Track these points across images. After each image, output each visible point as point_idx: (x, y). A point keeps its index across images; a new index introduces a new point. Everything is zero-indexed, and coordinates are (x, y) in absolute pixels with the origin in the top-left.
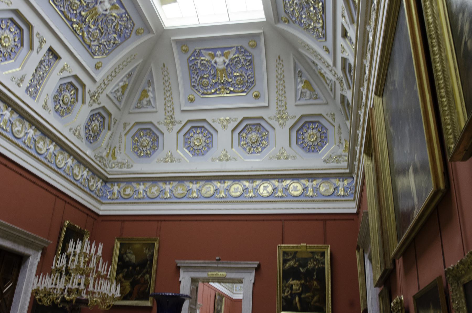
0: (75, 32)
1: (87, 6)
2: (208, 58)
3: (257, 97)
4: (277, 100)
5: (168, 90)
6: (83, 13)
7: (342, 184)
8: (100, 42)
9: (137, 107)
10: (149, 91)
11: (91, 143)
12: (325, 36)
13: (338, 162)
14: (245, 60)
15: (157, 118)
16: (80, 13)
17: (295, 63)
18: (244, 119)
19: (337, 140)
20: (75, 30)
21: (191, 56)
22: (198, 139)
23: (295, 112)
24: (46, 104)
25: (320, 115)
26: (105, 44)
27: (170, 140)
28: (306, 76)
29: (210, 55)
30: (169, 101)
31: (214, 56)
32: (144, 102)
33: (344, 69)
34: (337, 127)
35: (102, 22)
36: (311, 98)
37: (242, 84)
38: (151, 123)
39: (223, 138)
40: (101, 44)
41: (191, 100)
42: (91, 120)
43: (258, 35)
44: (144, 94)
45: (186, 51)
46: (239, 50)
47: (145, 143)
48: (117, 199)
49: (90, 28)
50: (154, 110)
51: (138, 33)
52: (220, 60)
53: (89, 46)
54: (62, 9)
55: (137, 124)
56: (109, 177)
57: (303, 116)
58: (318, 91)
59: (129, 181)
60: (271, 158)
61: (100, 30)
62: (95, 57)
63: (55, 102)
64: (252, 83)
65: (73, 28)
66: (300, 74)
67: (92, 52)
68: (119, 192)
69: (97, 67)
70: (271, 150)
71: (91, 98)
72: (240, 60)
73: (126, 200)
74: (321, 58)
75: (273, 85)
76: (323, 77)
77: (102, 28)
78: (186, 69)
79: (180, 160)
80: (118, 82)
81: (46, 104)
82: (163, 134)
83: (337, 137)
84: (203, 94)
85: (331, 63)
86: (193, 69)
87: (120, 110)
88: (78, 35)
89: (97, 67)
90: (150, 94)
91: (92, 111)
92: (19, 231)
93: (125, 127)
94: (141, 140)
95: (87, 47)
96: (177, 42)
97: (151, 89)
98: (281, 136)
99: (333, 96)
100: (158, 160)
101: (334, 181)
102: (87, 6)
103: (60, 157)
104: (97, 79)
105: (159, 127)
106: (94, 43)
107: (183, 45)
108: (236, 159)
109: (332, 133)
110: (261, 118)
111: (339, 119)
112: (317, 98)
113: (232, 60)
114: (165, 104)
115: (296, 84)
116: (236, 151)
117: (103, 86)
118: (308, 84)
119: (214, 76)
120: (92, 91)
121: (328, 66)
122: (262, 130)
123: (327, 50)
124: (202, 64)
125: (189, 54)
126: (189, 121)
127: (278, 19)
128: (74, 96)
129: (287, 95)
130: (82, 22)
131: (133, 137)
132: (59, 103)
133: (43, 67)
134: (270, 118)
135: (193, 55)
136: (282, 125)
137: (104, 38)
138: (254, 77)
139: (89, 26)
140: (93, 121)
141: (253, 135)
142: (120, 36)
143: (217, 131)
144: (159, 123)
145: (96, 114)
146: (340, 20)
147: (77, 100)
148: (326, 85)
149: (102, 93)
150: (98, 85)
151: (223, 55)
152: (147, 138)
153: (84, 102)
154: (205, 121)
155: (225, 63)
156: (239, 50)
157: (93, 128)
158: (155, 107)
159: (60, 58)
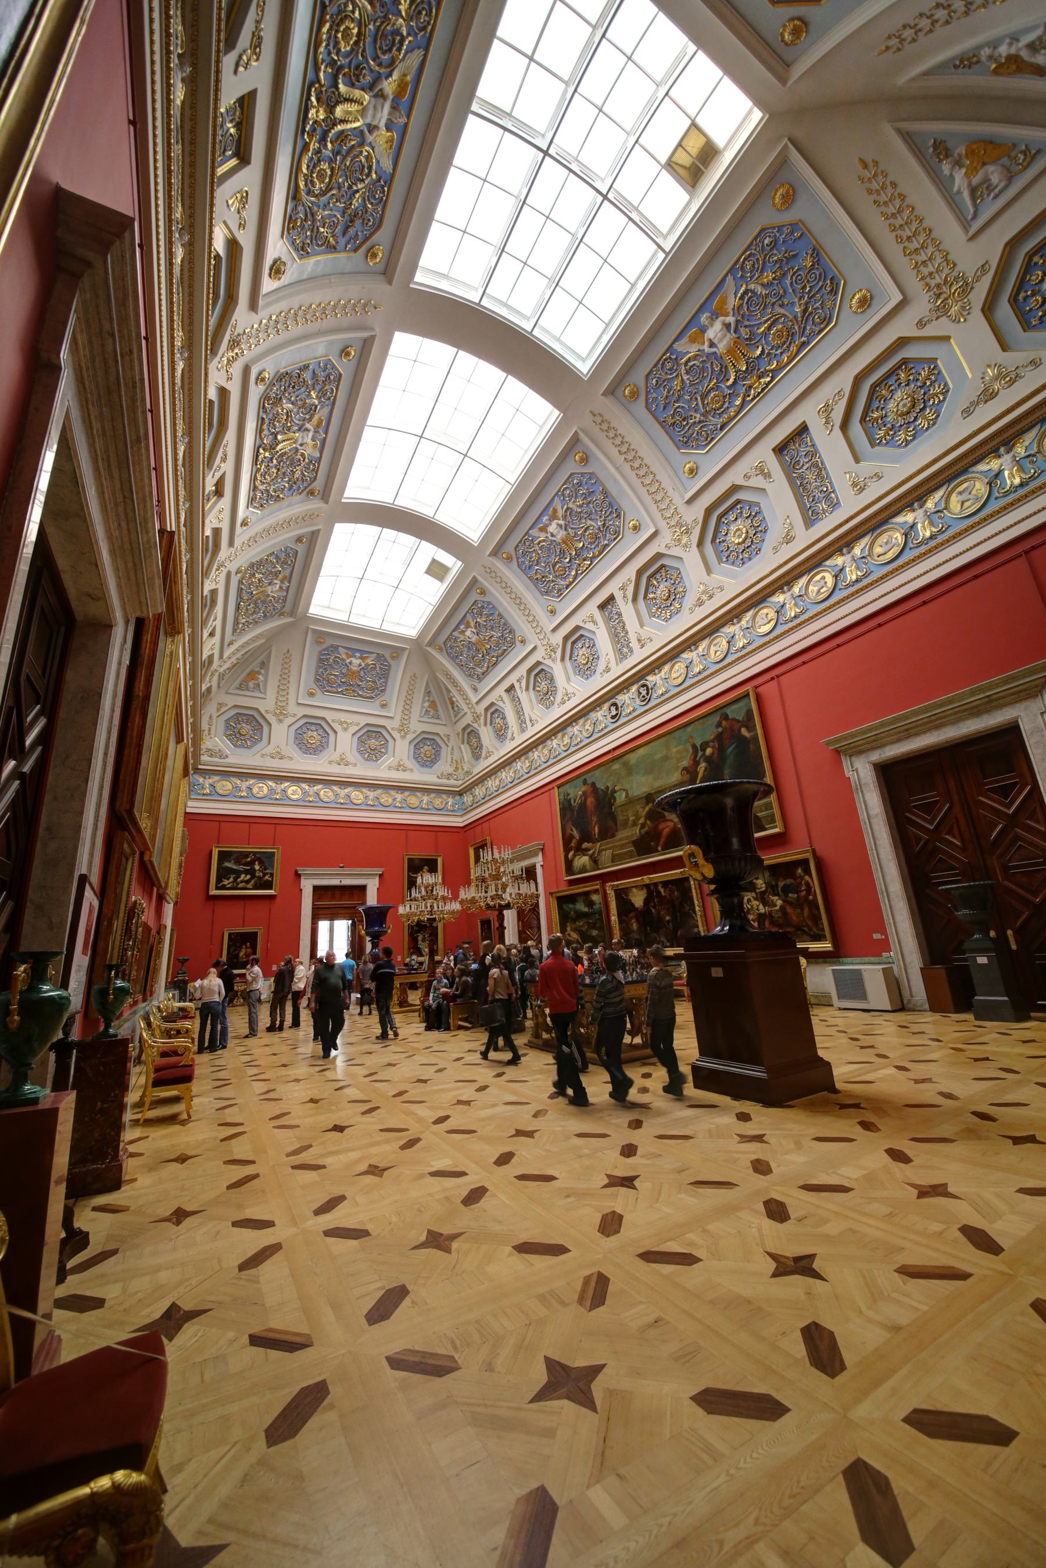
0: (238, 608)
2: (344, 657)
3: (383, 706)
4: (398, 709)
5: (284, 677)
7: (450, 801)
9: (240, 688)
10: (259, 673)
12: (480, 680)
13: (448, 779)
14: (381, 669)
15: (266, 704)
17: (427, 683)
18: (367, 725)
19: (449, 760)
21: (324, 650)
22: (313, 736)
23: (417, 727)
25: (438, 734)
27: (281, 734)
28: (435, 696)
29: (347, 654)
30: (282, 690)
31: (349, 656)
32: (251, 684)
33: (487, 709)
34: (450, 748)
36: (433, 717)
37: (372, 690)
38: (257, 710)
39: (345, 742)
41: (311, 695)
43: (403, 649)
44: (252, 675)
45: (318, 643)
46: (379, 657)
47: (243, 732)
48: (210, 795)
50: (262, 696)
51: (282, 614)
52: (356, 662)
55: (236, 706)
56: (200, 767)
57: (423, 732)
58: (441, 712)
59: (225, 774)
60: (390, 768)
64: (383, 691)
66: (428, 693)
68: (212, 786)
69: (231, 643)
70: (388, 760)
72: (375, 668)
73: (223, 798)
74: (461, 691)
75: (402, 698)
76: (452, 703)
78: (314, 663)
79: (291, 758)
80: (234, 660)
82: (270, 724)
83: (449, 756)
84: (327, 691)
85: (474, 700)
86: (322, 662)
87: (219, 687)
90: (261, 677)
93: (218, 710)
94: (239, 726)
96: (315, 631)
97: (263, 671)
98: (401, 749)
99: (454, 720)
100: (263, 756)
101: (444, 796)
104: (225, 656)
105: (267, 716)
107: (320, 637)
108: (355, 765)
109: (445, 752)
110: (384, 727)
111: (454, 741)
112: (438, 718)
113: (368, 665)
114: (278, 692)
115: (424, 702)
116: (353, 756)
118: (433, 704)
119: (345, 675)
121: (466, 699)
122: (381, 739)
123: (475, 690)
124: (334, 661)
125: (324, 646)
126: (305, 716)
127: (430, 644)
129: (412, 710)
131: (227, 721)
134: (392, 729)
135: (326, 649)
136: (403, 737)
138: (385, 686)
141: (373, 743)
142: (265, 616)
143: (336, 732)
144: (267, 711)
146: (512, 679)
148: (451, 711)
151: (361, 658)
152: (247, 727)
154: (324, 719)
155: (360, 665)
156: (379, 657)
158: (265, 693)
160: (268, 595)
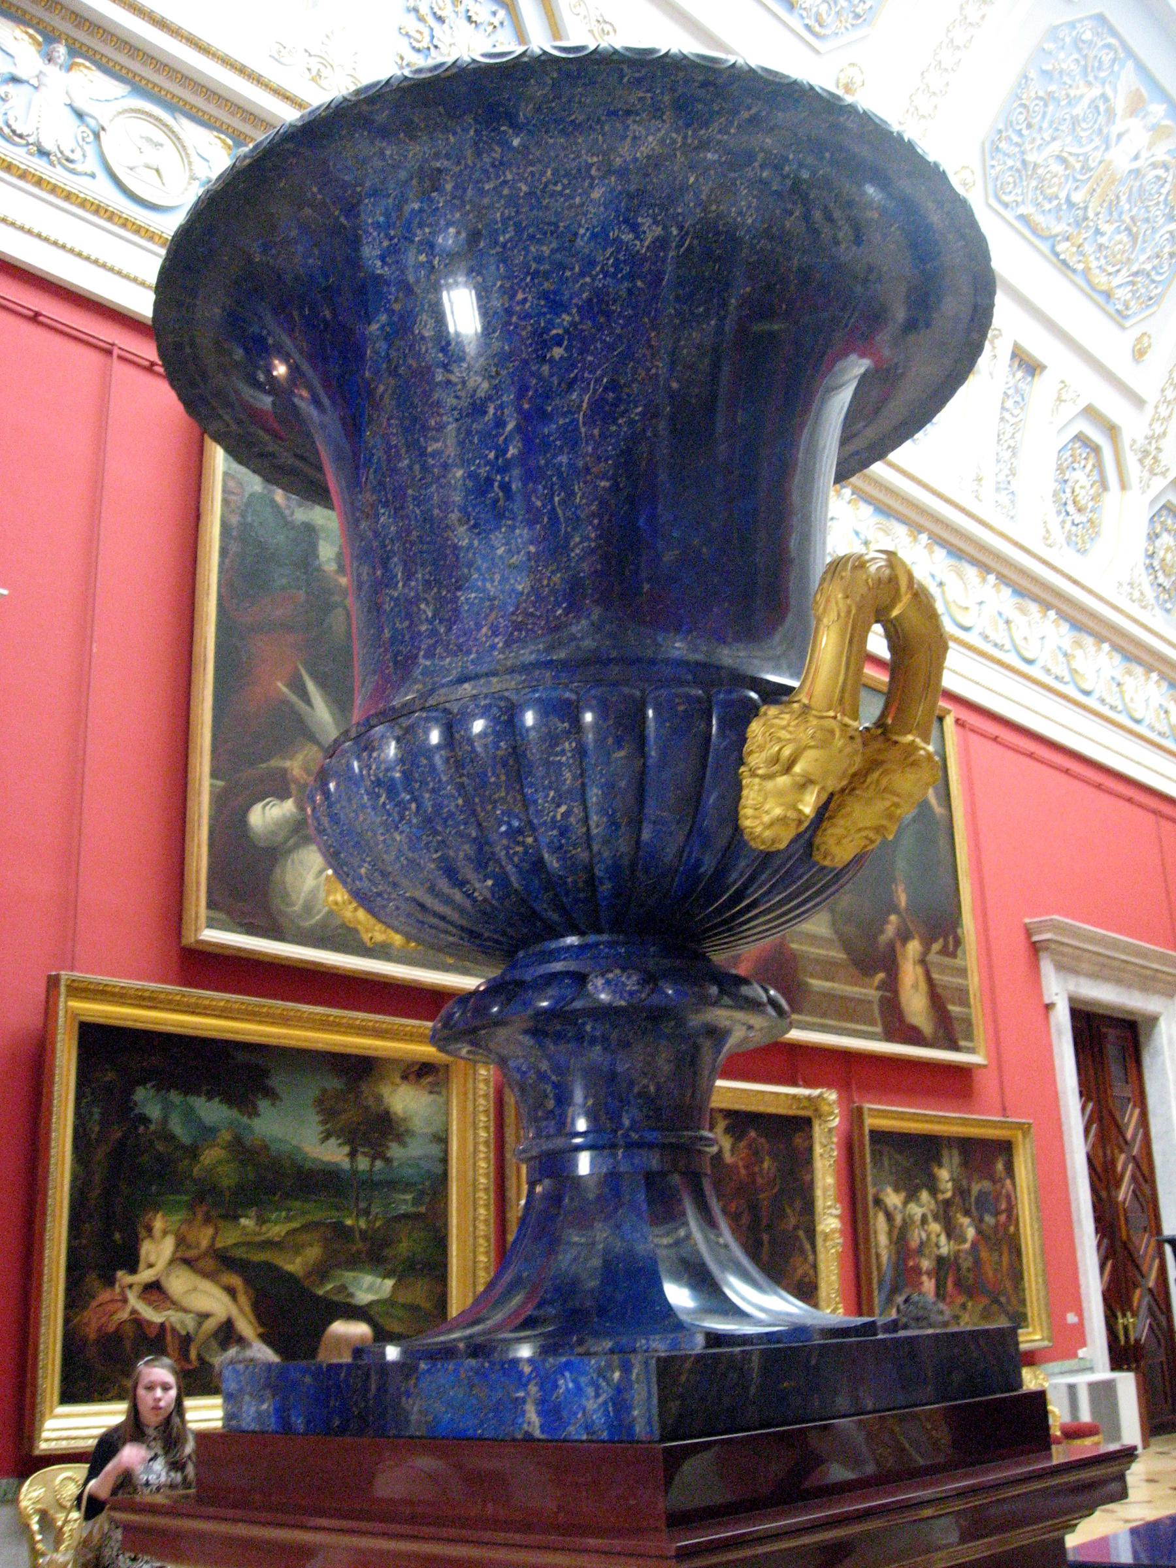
1: (1085, 168)
6: (1077, 197)
8: (1135, 268)
11: (1168, 611)
16: (1070, 204)
20: (1064, 262)
24: (1048, 531)
26: (1148, 267)
35: (1129, 200)
40: (1136, 274)
42: (1153, 536)
49: (1103, 234)
53: (1108, 295)
54: (1022, 210)
61: (1127, 229)
62: (1127, 324)
63: (1059, 513)
65: (1057, 255)
67: (1118, 311)
69: (1139, 353)
71: (1141, 461)
77: (1132, 218)
81: (1048, 531)
88: (1074, 271)
89: (1139, 353)
91: (1153, 502)
92: (1126, 949)
95: (1101, 300)
102: (1085, 168)
103: (1129, 683)
106: (1117, 281)
117: (1164, 411)
120: (1141, 441)
128: (1095, 476)
130: (1078, 224)
132: (1068, 514)
133: (1007, 415)
137: (1143, 250)
139: (1098, 232)
140: (1157, 536)
145: (1158, 513)
147: (1104, 486)
149: (1164, 433)
150: (1149, 410)
153: (1124, 486)
157: (1163, 560)
159: (1043, 368)
160: (1137, 173)
